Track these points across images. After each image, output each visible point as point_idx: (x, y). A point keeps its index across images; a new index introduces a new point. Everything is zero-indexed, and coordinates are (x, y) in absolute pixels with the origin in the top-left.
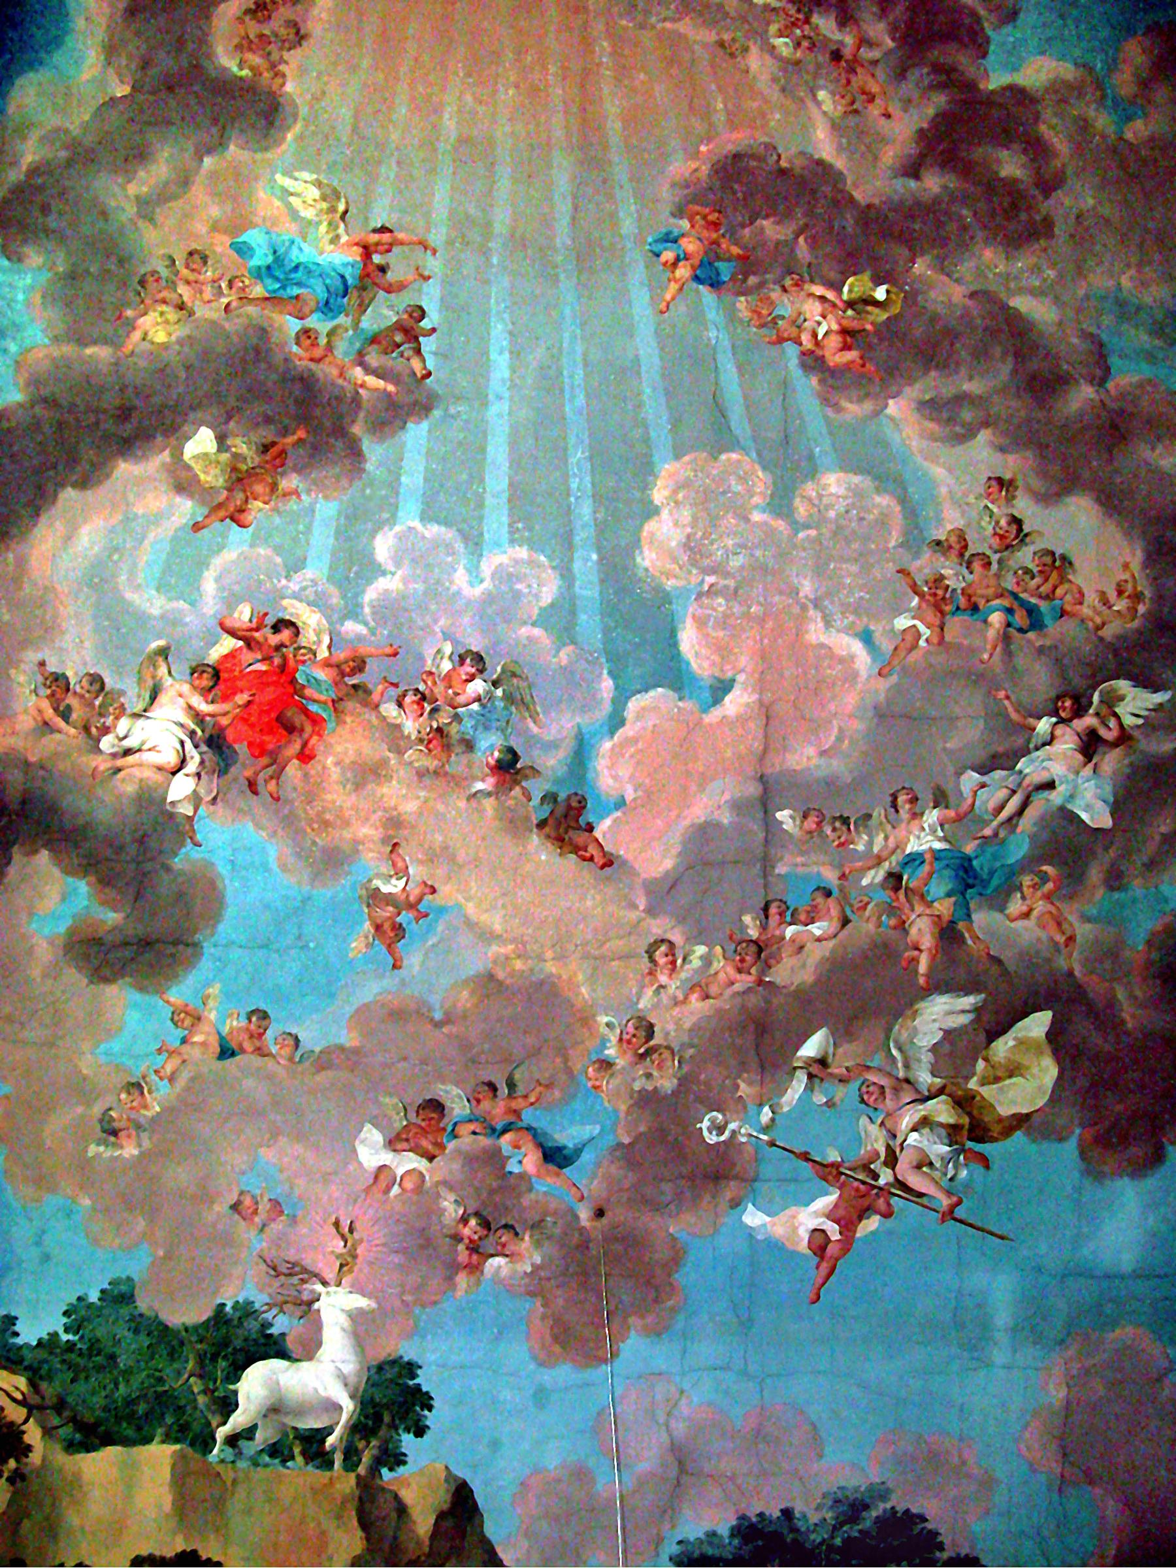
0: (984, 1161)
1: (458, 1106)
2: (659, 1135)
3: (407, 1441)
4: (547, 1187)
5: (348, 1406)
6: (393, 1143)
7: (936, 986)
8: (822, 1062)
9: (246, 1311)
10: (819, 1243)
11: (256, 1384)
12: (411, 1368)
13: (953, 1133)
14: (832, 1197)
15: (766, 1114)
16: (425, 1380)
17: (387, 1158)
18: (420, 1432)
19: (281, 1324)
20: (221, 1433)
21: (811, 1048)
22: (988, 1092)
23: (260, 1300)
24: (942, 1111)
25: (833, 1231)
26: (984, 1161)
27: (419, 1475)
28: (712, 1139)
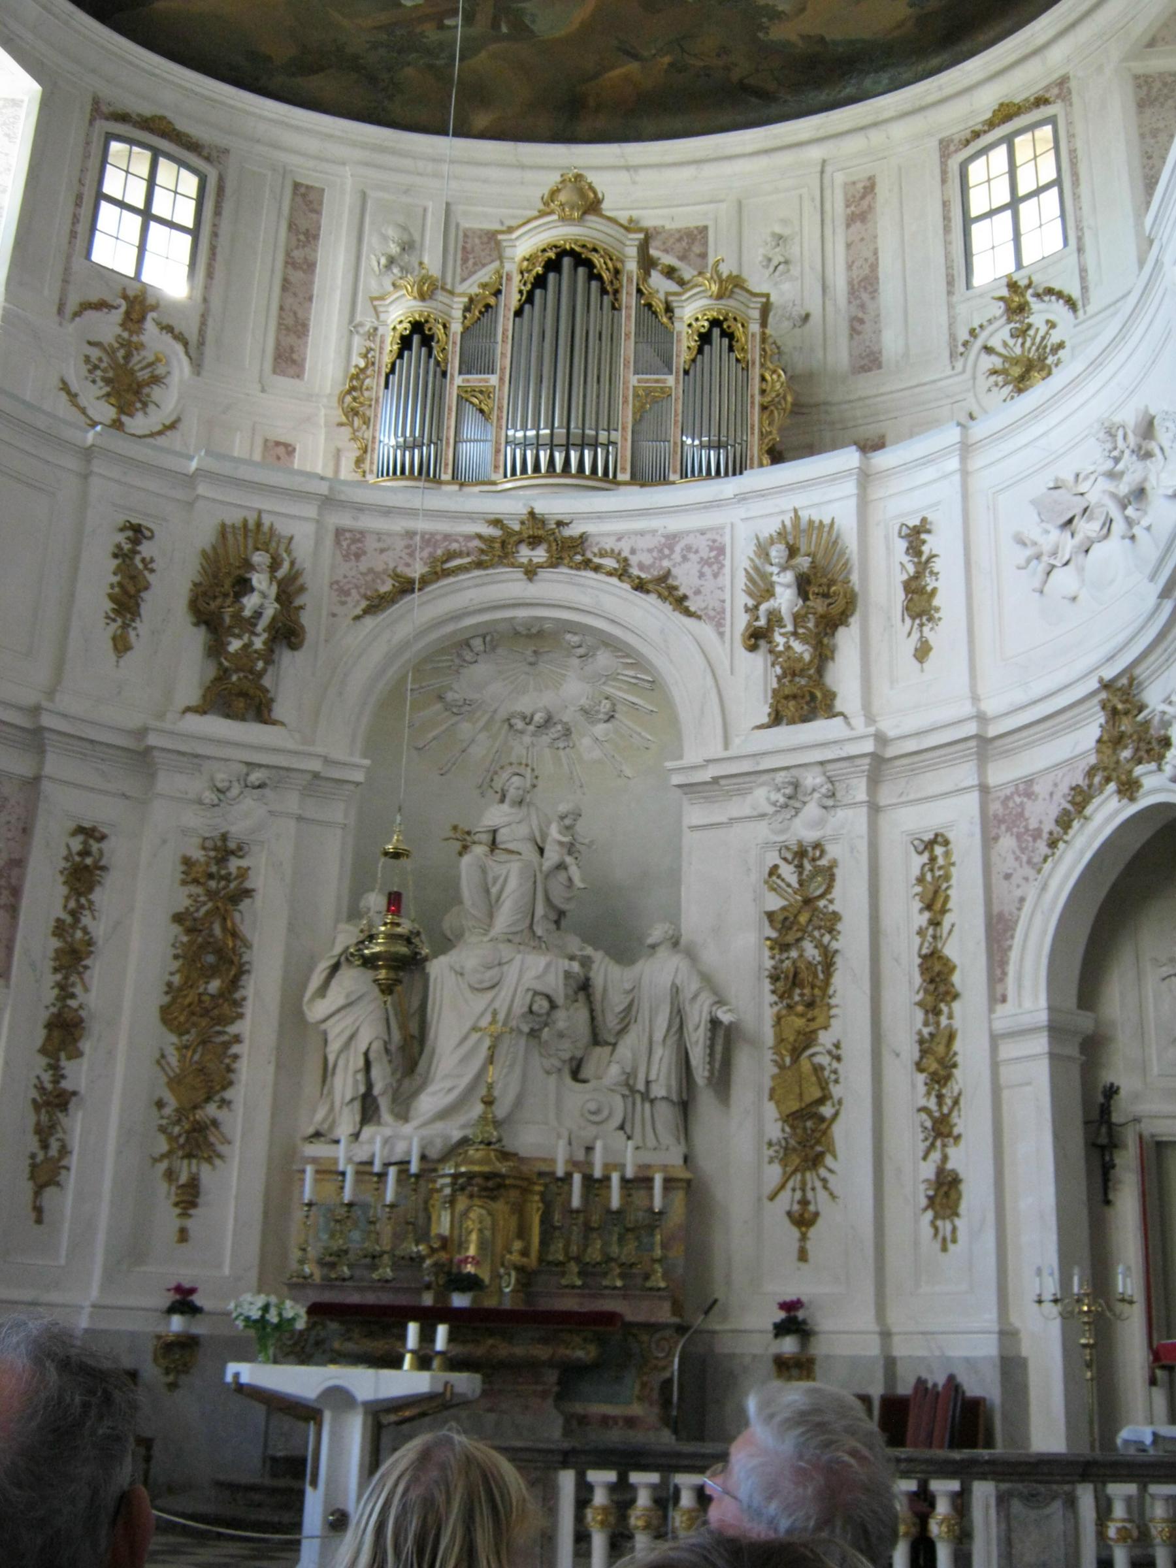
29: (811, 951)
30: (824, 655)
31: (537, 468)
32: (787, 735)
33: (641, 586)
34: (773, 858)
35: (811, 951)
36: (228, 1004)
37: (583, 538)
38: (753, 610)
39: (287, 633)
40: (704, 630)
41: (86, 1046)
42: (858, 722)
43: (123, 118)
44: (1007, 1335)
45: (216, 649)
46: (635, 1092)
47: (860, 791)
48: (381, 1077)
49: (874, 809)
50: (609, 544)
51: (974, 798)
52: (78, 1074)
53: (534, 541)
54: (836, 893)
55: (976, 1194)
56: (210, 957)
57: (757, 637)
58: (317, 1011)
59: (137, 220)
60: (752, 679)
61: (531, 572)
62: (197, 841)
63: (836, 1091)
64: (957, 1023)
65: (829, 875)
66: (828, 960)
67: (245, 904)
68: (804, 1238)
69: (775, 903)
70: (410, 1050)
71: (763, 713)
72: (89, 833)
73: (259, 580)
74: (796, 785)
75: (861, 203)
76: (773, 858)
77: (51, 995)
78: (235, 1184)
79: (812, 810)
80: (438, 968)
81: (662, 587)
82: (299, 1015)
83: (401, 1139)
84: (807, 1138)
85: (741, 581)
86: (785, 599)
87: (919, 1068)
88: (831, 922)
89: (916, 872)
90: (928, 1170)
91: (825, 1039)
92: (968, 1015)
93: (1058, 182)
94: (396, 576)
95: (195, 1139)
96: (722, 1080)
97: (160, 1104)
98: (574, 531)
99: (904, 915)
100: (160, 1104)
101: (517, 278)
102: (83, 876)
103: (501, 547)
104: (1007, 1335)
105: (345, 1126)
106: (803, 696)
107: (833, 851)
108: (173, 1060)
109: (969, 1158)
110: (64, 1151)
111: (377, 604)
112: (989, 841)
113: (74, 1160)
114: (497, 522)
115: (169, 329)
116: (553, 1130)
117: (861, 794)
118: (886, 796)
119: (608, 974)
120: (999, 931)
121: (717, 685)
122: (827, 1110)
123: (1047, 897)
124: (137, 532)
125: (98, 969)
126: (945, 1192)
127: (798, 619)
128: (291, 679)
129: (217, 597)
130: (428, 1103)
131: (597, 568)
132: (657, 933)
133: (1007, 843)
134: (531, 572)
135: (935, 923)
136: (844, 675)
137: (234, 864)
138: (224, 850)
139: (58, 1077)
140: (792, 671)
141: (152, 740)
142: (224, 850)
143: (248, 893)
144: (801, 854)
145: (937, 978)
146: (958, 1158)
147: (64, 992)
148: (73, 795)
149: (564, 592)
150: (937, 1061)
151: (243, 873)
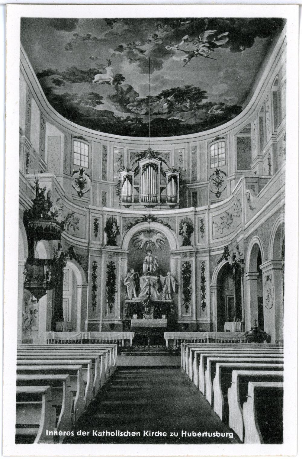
0: (213, 51)
1: (125, 45)
2: (159, 49)
3: (122, 82)
4: (140, 55)
5: (112, 79)
6: (115, 50)
7: (208, 29)
8: (187, 39)
9: (94, 69)
10: (185, 60)
11: (97, 77)
12: (121, 75)
13: (208, 47)
14: (188, 55)
15: (177, 46)
16: (124, 76)
17: (114, 52)
18: (124, 81)
19: (100, 71)
20: (93, 81)
21: (186, 37)
22: (215, 42)
23: (96, 68)
24: (207, 45)
25: (187, 59)
26: (213, 51)
27: (124, 85)
28: (168, 49)
29: (188, 275)
30: (190, 237)
31: (146, 201)
32: (184, 247)
33: (165, 225)
34: (183, 263)
35: (188, 275)
36: (114, 284)
37: (156, 218)
38: (180, 230)
39: (118, 233)
40: (174, 233)
41: (97, 289)
42: (194, 246)
43: (75, 137)
44: (211, 320)
45: (108, 236)
46: (166, 293)
47: (194, 255)
48: (134, 292)
49: (196, 257)
50: (160, 219)
51: (208, 257)
52: (96, 293)
53: (150, 219)
54: (191, 268)
55: (208, 304)
57: (180, 234)
58: (126, 284)
59: (79, 155)
60: (181, 239)
61: (149, 222)
62: (108, 262)
63: (191, 293)
64: (206, 285)
65: (190, 266)
66: (190, 277)
67: (115, 270)
68: (187, 310)
69: (183, 269)
71: (182, 244)
72: (95, 262)
73: (115, 228)
74: (186, 254)
76: (183, 263)
77: (92, 283)
79: (188, 258)
80: (141, 279)
81: (167, 225)
82: (123, 284)
84: (187, 299)
85: (179, 226)
86: (185, 228)
87: (201, 290)
88: (190, 272)
89: (201, 266)
90: (202, 302)
91: (190, 286)
93: (225, 153)
94: (131, 224)
95: (111, 300)
96: (177, 291)
97: (107, 296)
98: (155, 217)
99: (200, 271)
100: (107, 296)
101: (142, 168)
102: (94, 268)
103: (145, 219)
104: (211, 320)
105: (130, 297)
106: (187, 242)
107: (191, 263)
108: (108, 290)
109: (207, 301)
110: (96, 302)
111: (129, 228)
112: (210, 262)
113: (97, 303)
114: (144, 216)
115: (86, 174)
117: (194, 256)
118: (198, 255)
119: (162, 278)
120: (211, 273)
122: (190, 295)
124: (96, 220)
125: (98, 280)
126: (204, 305)
127: (186, 232)
128: (118, 239)
130: (141, 295)
131: (158, 222)
132: (169, 273)
133: (212, 263)
134: (149, 222)
135: (203, 272)
136: (192, 239)
137: (113, 265)
138: (112, 263)
139: (94, 293)
140: (185, 239)
141: (102, 250)
142: (112, 263)
143: (115, 269)
144: (186, 263)
145: (203, 279)
146: (205, 301)
147: (94, 283)
150: (203, 289)
151: (114, 266)
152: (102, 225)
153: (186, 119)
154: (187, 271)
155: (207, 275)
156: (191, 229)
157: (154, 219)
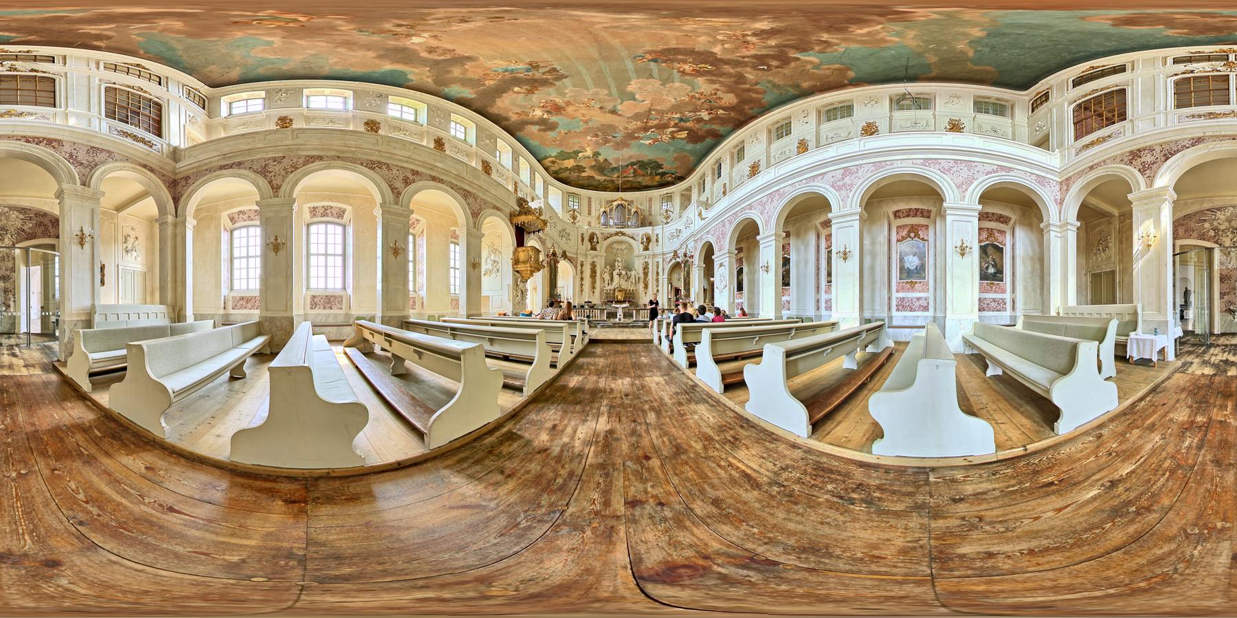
27: (601, 158)
56: (593, 272)
60: (641, 247)
70: (612, 279)
75: (650, 200)
78: (597, 291)
83: (612, 287)
84: (646, 286)
92: (660, 277)
103: (617, 234)
106: (646, 249)
116: (625, 285)
121: (638, 247)
123: (668, 267)
128: (598, 247)
129: (591, 239)
148: (580, 259)
149: (623, 238)
150: (657, 280)
152: (586, 239)
153: (646, 181)
154: (646, 268)
155: (660, 271)
156: (649, 240)
157: (623, 234)
